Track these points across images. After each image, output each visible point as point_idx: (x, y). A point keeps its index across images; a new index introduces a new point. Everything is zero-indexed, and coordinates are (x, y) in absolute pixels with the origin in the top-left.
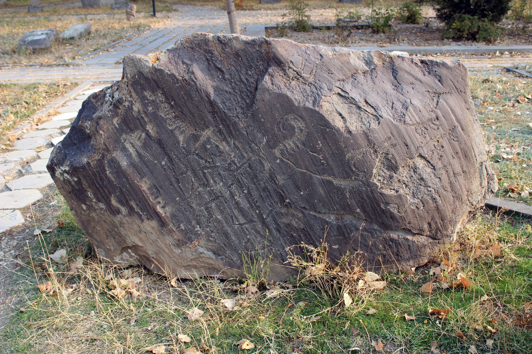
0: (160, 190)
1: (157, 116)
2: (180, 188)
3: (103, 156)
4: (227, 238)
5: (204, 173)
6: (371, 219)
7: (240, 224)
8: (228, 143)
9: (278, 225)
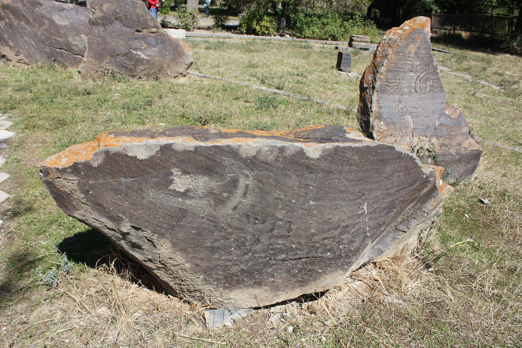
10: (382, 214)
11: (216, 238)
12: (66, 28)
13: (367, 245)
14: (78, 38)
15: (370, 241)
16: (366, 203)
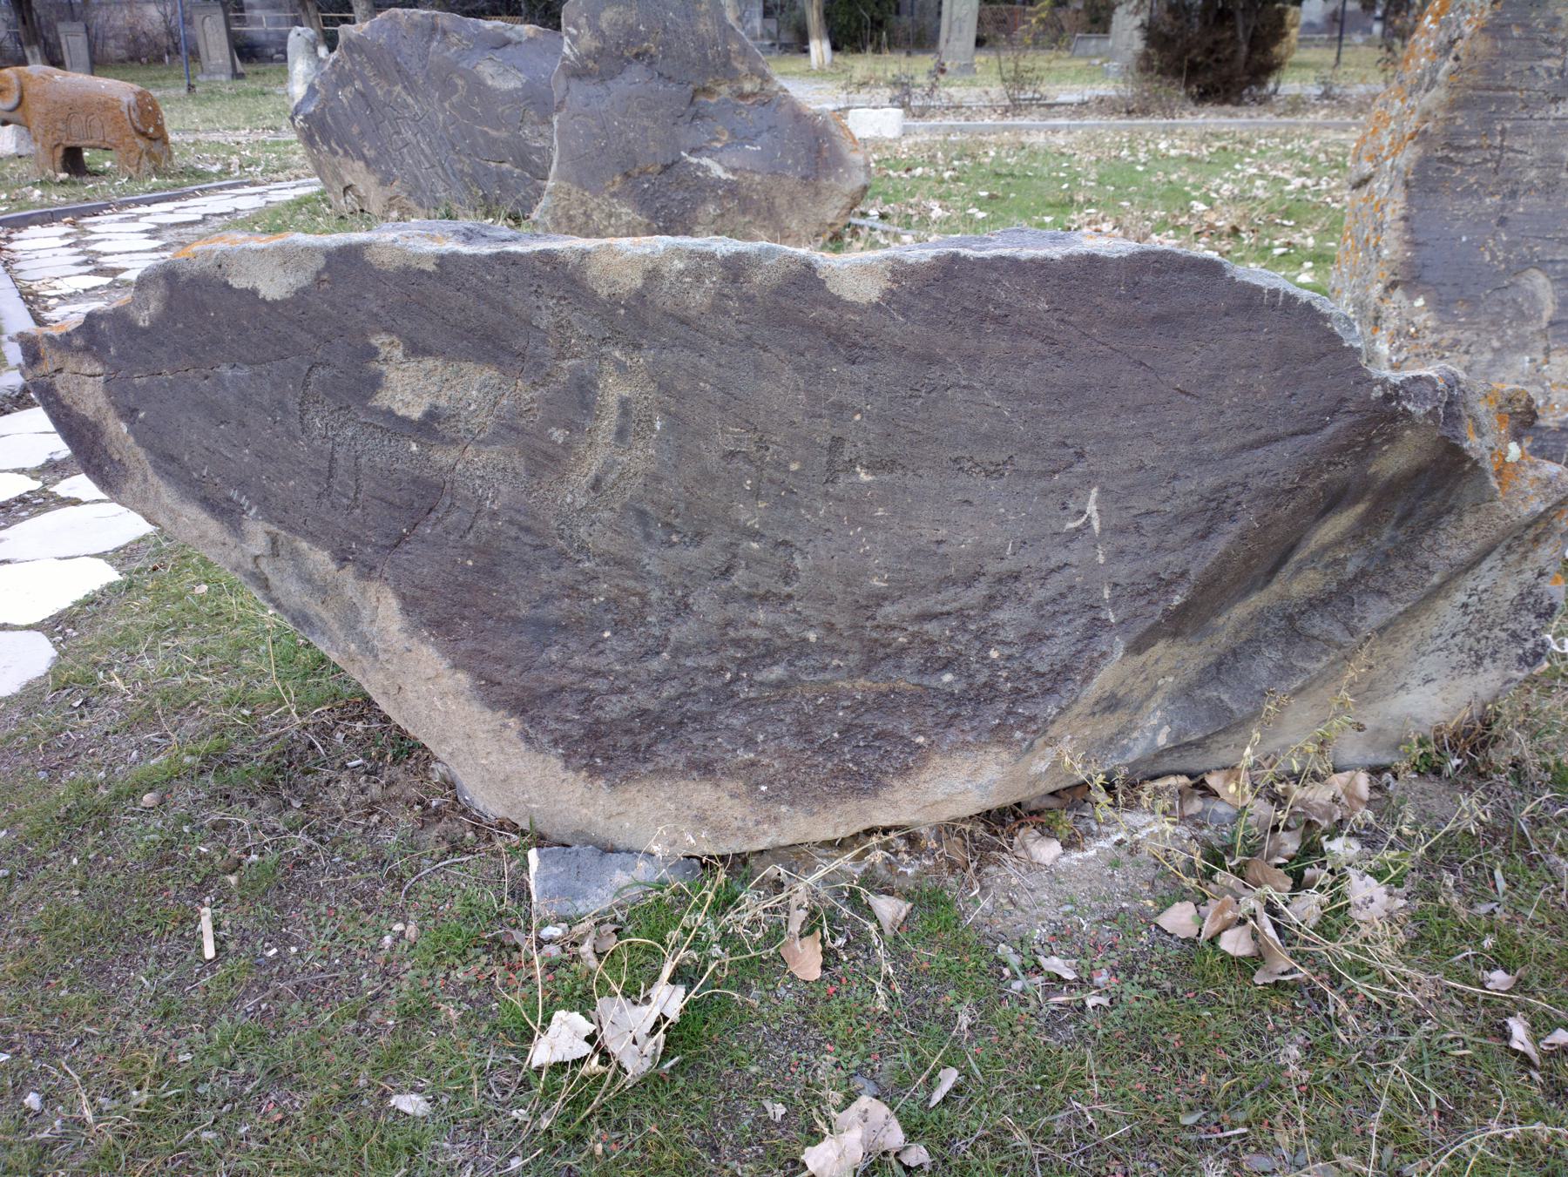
10: (1172, 540)
11: (545, 589)
13: (1103, 655)
15: (1120, 645)
16: (1094, 492)
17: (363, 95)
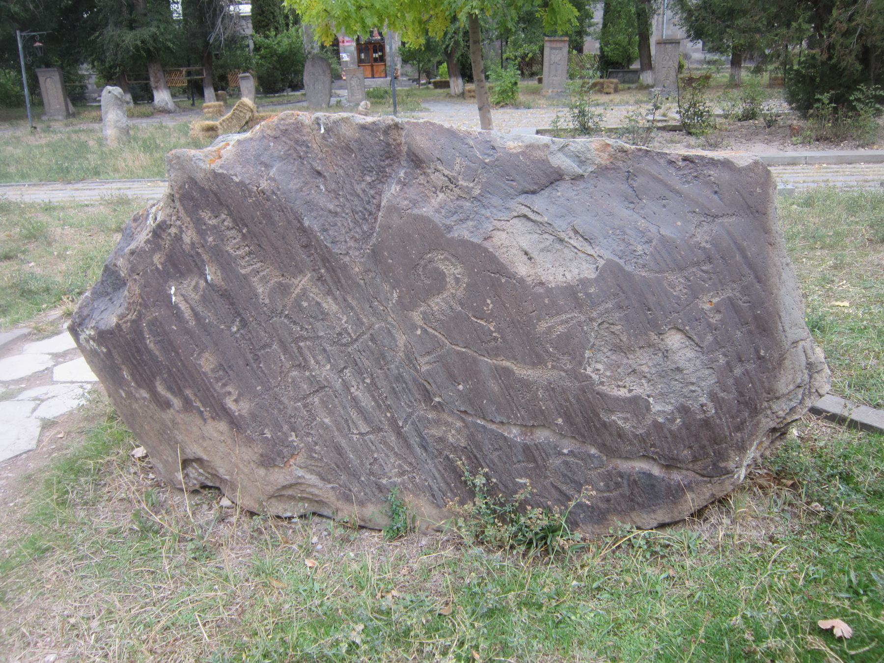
0: (230, 372)
1: (221, 251)
2: (262, 371)
3: (140, 316)
4: (340, 454)
5: (299, 348)
6: (583, 436)
7: (361, 434)
8: (335, 299)
9: (424, 438)
12: (579, 305)
14: (644, 361)
17: (225, 295)
